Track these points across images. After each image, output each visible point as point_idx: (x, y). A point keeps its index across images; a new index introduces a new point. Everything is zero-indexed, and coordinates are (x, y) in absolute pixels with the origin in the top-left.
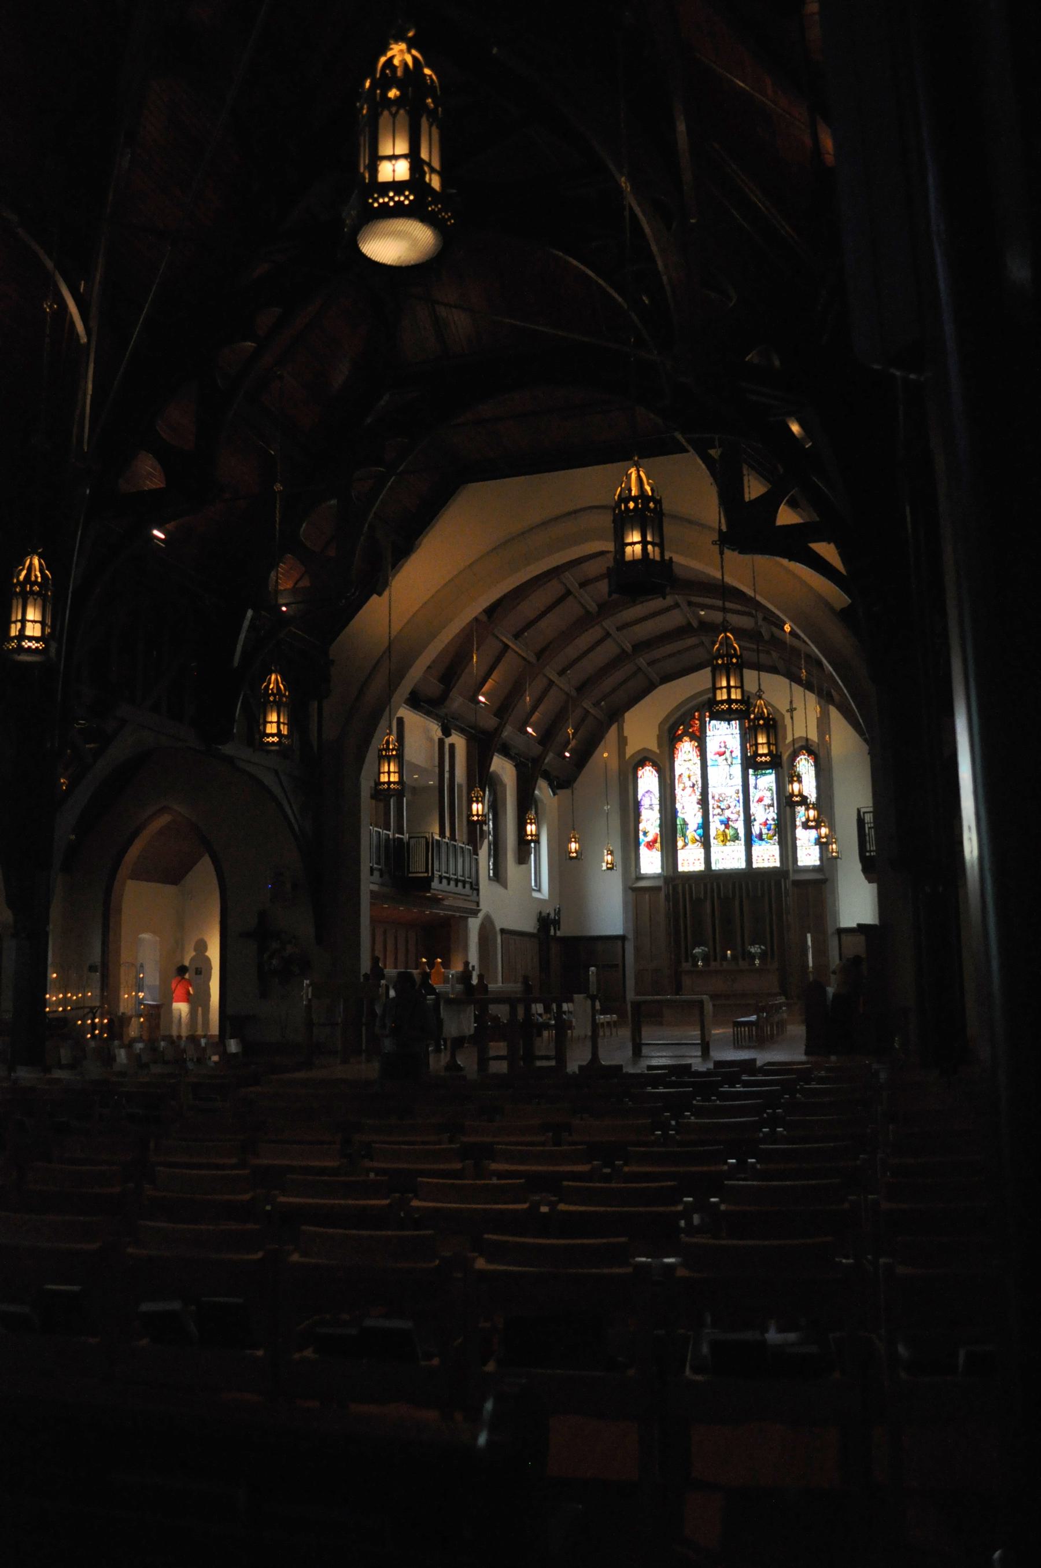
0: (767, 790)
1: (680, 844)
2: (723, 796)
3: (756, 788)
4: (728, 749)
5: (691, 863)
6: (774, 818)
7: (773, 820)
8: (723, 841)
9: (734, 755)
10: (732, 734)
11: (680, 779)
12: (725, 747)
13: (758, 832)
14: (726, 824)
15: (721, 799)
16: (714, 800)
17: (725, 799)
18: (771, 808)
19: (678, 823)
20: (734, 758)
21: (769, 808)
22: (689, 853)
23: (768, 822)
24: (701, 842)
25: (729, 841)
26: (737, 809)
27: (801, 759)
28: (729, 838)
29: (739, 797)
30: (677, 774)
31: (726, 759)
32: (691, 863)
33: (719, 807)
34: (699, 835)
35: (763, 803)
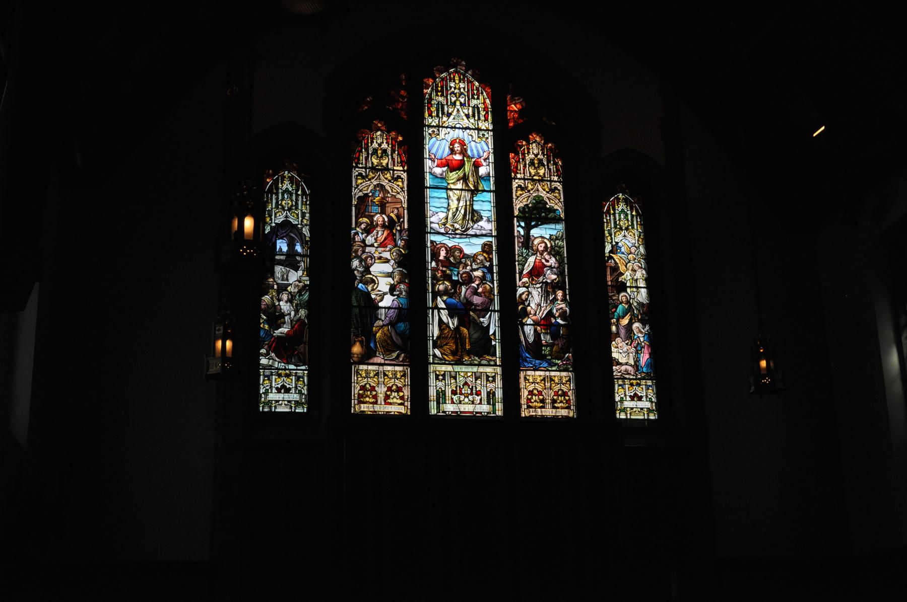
0: (549, 254)
1: (357, 349)
2: (457, 253)
3: (527, 242)
4: (468, 157)
5: (381, 397)
6: (566, 311)
7: (563, 315)
8: (454, 353)
9: (482, 171)
10: (479, 129)
11: (363, 208)
12: (463, 152)
13: (531, 339)
14: (463, 311)
15: (452, 259)
16: (438, 261)
17: (461, 263)
18: (560, 294)
19: (354, 303)
20: (481, 178)
21: (554, 293)
22: (377, 374)
23: (553, 321)
24: (402, 351)
25: (469, 353)
26: (488, 286)
27: (618, 199)
28: (468, 347)
29: (491, 260)
30: (356, 193)
31: (465, 179)
32: (381, 397)
33: (447, 277)
34: (400, 334)
35: (541, 279)
